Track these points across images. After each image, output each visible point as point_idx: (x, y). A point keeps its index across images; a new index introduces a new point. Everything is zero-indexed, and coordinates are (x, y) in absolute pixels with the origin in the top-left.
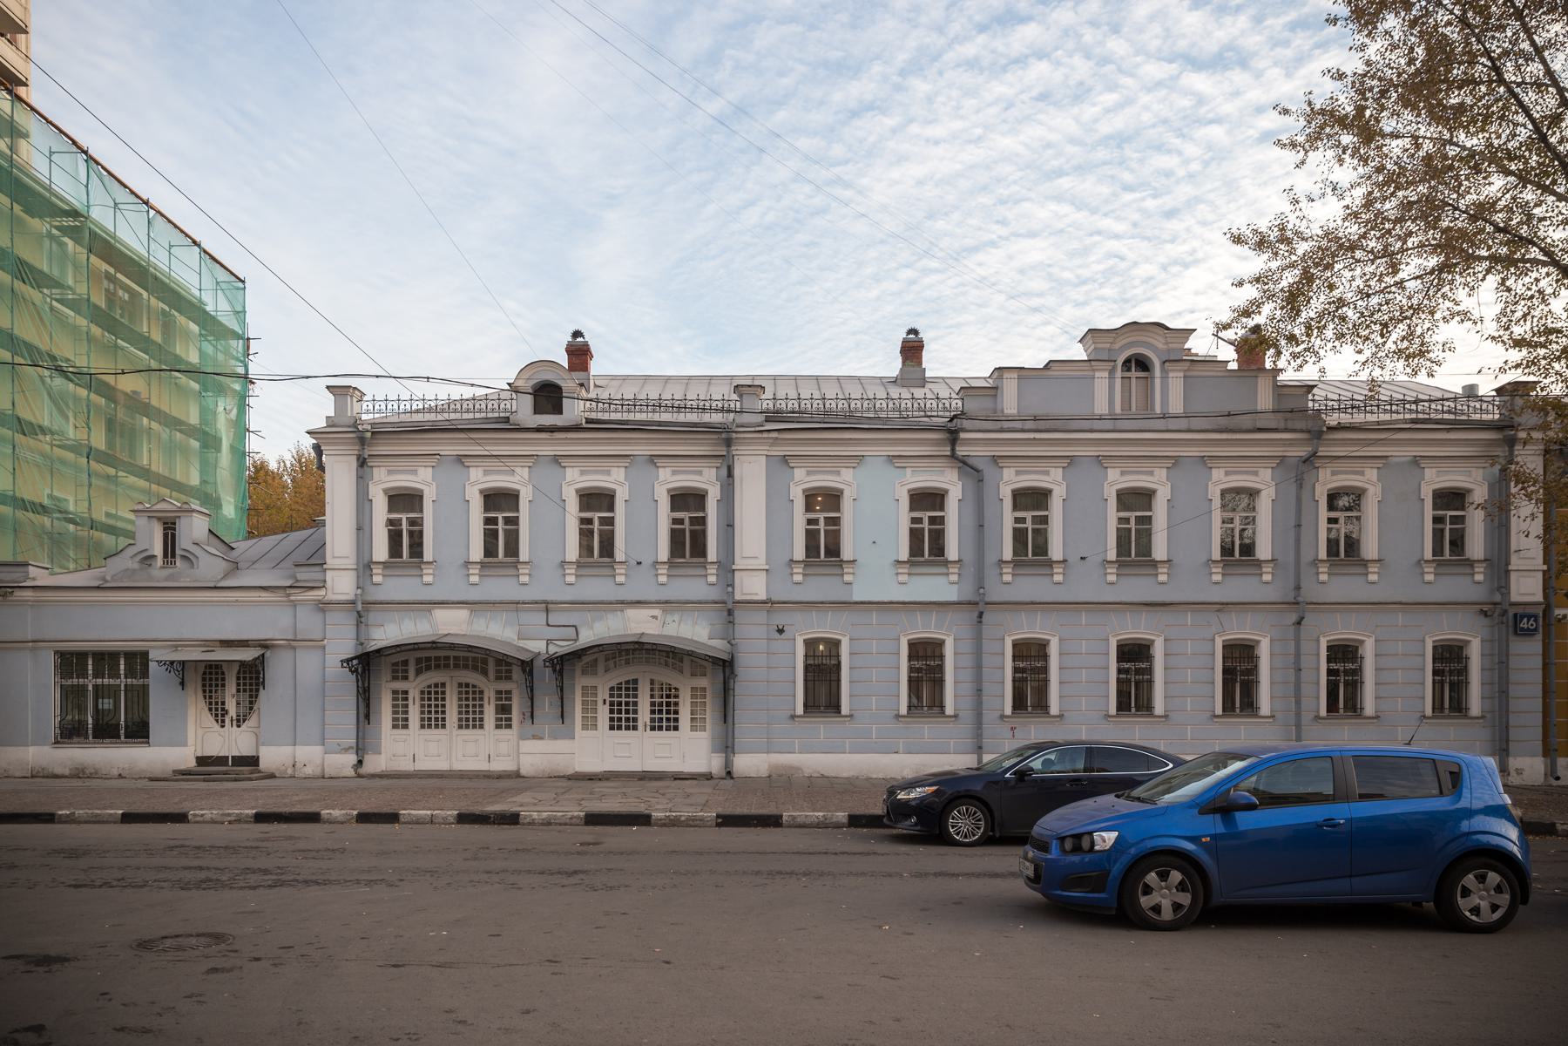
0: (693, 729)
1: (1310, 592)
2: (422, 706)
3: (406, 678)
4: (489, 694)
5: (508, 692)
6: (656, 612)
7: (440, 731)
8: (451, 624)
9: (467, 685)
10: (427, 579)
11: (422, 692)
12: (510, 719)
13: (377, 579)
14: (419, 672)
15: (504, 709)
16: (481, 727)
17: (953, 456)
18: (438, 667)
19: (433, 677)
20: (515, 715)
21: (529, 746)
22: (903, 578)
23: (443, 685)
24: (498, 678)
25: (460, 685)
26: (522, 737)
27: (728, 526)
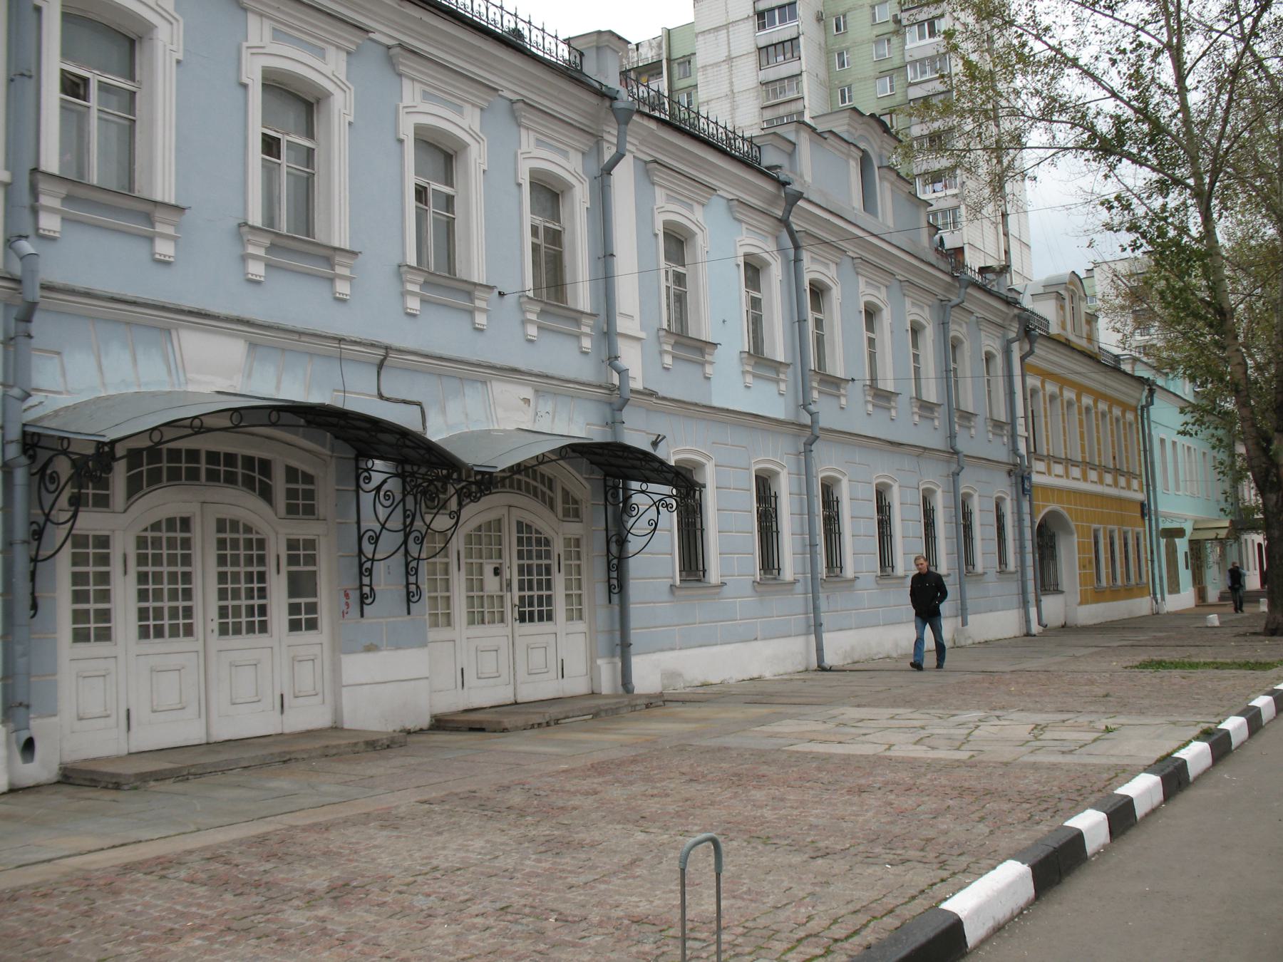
0: (570, 618)
1: (963, 445)
2: (142, 578)
3: (103, 502)
4: (277, 548)
5: (310, 544)
6: (528, 392)
7: (182, 643)
8: (214, 373)
9: (235, 525)
10: (164, 248)
11: (141, 542)
12: (312, 608)
13: (49, 223)
14: (134, 487)
15: (301, 585)
16: (264, 628)
17: (784, 222)
18: (174, 476)
19: (166, 502)
20: (326, 599)
21: (358, 667)
22: (749, 379)
23: (186, 523)
24: (292, 510)
25: (221, 525)
26: (341, 647)
27: (605, 256)
